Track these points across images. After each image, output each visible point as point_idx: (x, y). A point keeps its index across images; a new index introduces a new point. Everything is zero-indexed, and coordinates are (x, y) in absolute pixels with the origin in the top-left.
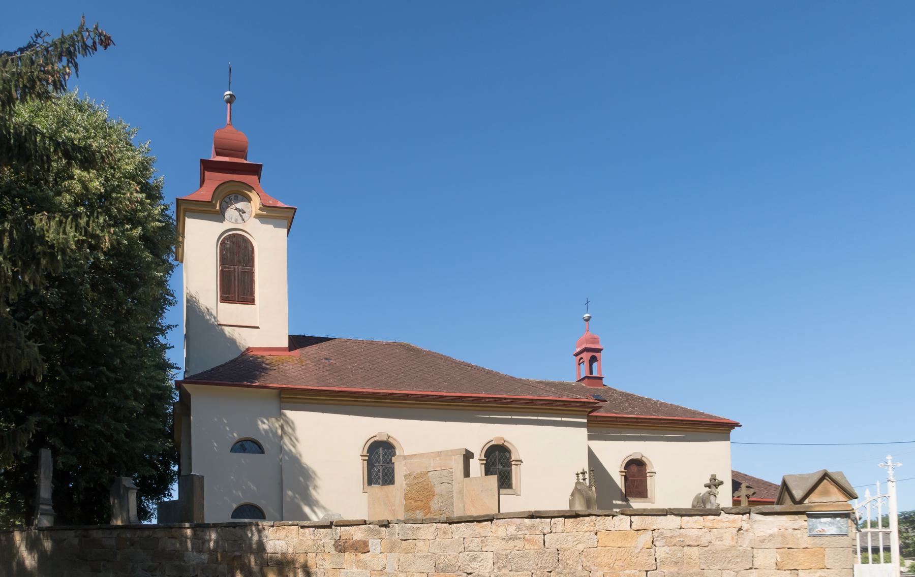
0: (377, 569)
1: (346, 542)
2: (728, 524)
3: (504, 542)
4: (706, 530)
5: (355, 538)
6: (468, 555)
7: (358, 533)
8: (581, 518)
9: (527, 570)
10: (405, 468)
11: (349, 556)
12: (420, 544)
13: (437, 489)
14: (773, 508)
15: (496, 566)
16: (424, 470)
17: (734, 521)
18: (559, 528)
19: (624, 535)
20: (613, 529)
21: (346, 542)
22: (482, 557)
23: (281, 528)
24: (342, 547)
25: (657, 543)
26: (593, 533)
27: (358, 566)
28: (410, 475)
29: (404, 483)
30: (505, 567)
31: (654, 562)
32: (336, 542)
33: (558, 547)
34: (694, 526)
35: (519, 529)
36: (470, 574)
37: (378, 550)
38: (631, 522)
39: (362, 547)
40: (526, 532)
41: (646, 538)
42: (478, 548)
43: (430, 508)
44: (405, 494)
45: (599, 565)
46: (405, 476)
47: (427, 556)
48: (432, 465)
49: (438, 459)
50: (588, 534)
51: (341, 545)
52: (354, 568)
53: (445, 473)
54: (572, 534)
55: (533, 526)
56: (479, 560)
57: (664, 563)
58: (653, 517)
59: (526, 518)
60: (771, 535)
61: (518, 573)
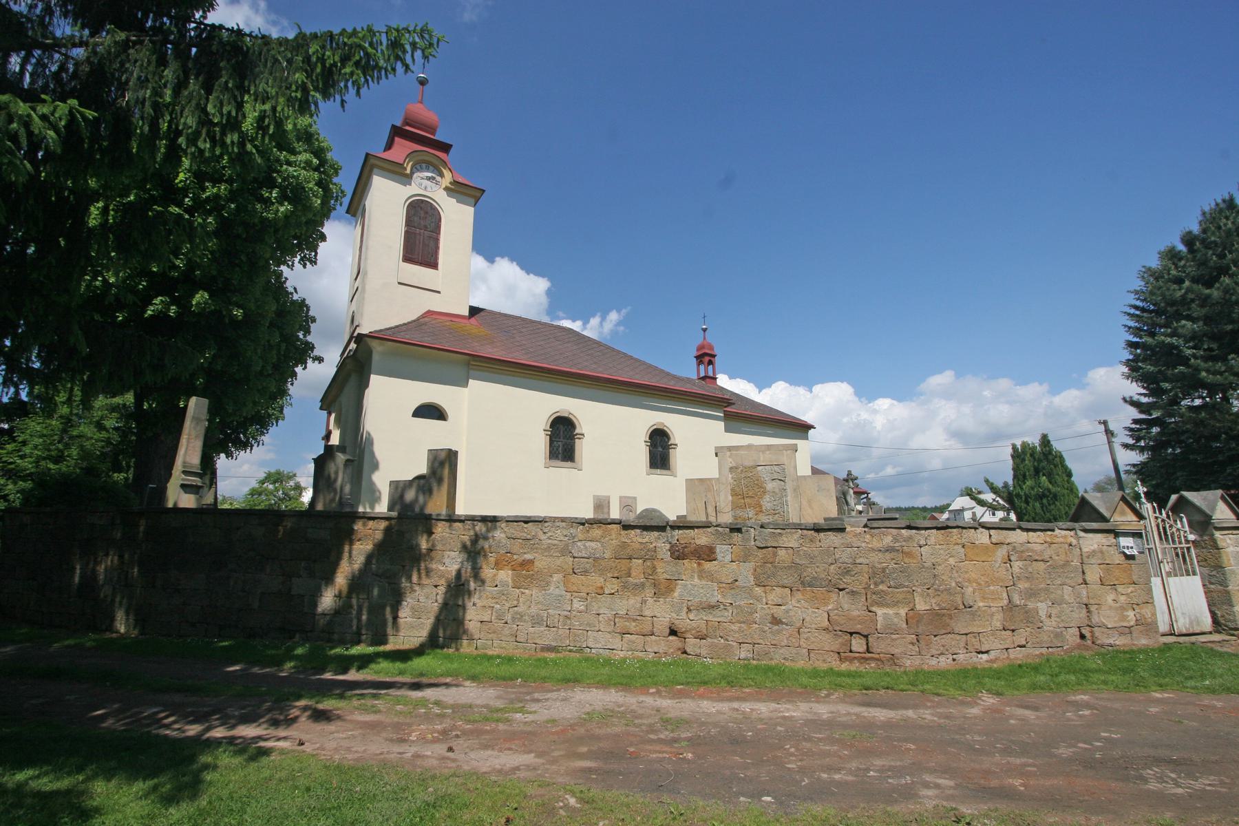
0: (727, 581)
1: (686, 547)
2: (1061, 540)
3: (880, 555)
4: (1046, 545)
5: (698, 542)
6: (840, 568)
7: (701, 538)
8: (950, 530)
9: (907, 587)
10: (731, 460)
11: (689, 564)
12: (781, 553)
13: (770, 486)
14: (1088, 526)
15: (872, 581)
16: (752, 464)
17: (1065, 537)
18: (932, 540)
19: (985, 549)
20: (977, 542)
21: (686, 547)
22: (856, 570)
23: (595, 526)
24: (679, 554)
25: (1012, 558)
26: (960, 546)
27: (700, 577)
28: (736, 468)
29: (730, 476)
30: (882, 582)
31: (1011, 577)
32: (672, 547)
33: (933, 561)
34: (1038, 541)
35: (895, 540)
36: (843, 589)
37: (728, 558)
38: (990, 536)
39: (707, 554)
40: (904, 543)
41: (1002, 552)
42: (851, 560)
43: (761, 506)
44: (732, 490)
45: (969, 581)
46: (731, 468)
47: (790, 567)
48: (762, 459)
49: (768, 452)
50: (956, 547)
51: (678, 551)
52: (696, 580)
53: (776, 468)
54: (944, 547)
55: (910, 538)
56: (853, 573)
57: (1019, 578)
58: (1004, 532)
59: (903, 528)
60: (1094, 551)
61: (898, 590)
